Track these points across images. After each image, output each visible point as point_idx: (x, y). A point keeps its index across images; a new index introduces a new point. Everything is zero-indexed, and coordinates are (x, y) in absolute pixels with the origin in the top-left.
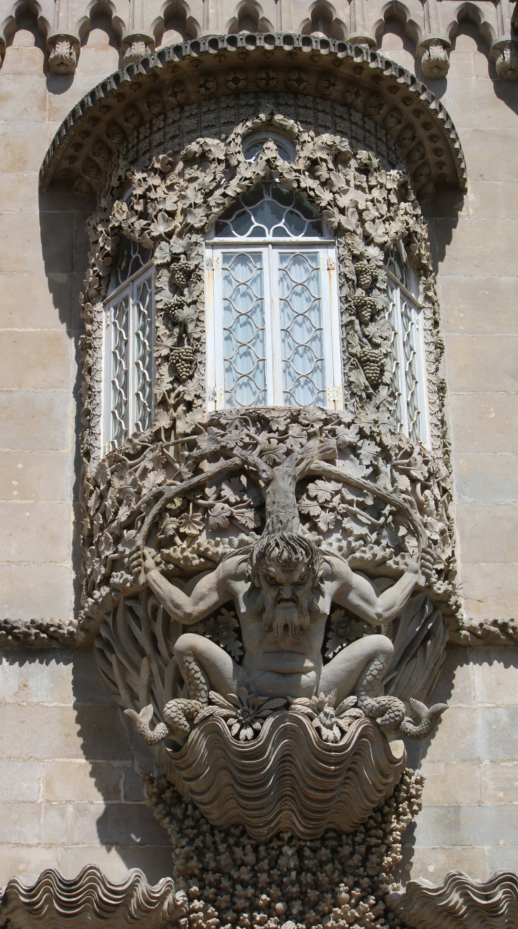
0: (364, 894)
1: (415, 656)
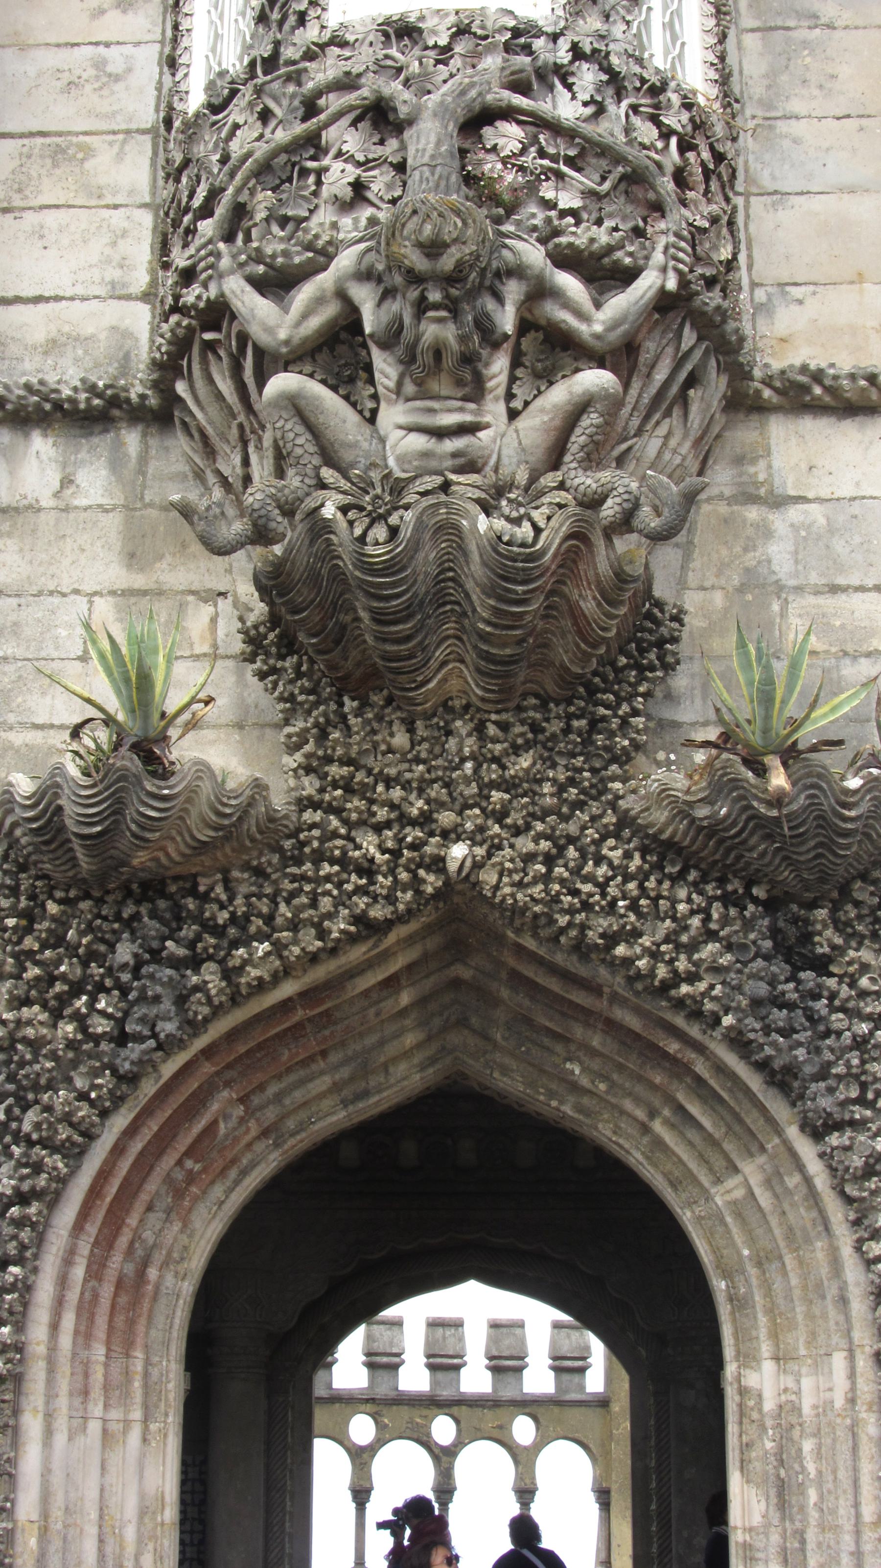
0: (582, 797)
1: (668, 414)
